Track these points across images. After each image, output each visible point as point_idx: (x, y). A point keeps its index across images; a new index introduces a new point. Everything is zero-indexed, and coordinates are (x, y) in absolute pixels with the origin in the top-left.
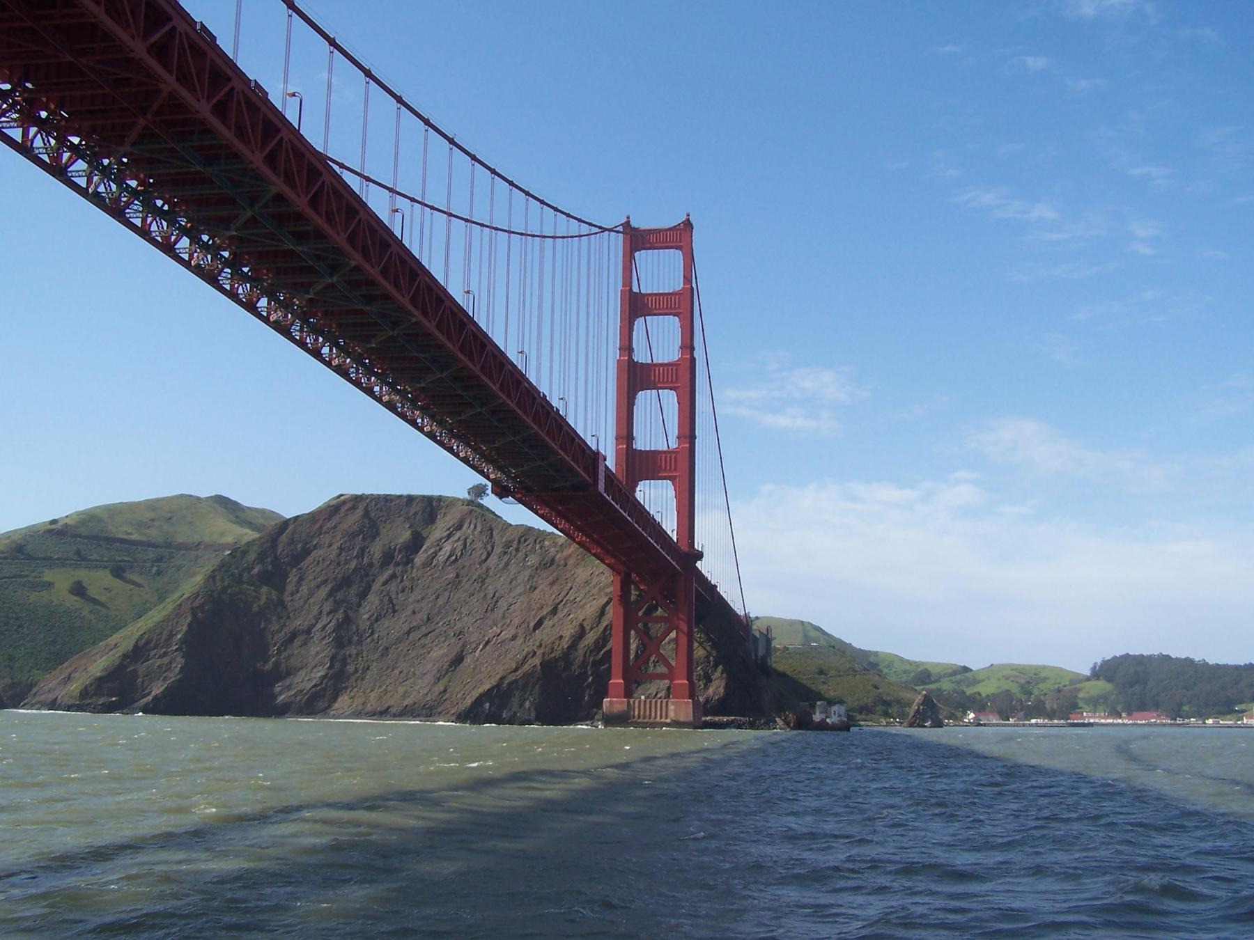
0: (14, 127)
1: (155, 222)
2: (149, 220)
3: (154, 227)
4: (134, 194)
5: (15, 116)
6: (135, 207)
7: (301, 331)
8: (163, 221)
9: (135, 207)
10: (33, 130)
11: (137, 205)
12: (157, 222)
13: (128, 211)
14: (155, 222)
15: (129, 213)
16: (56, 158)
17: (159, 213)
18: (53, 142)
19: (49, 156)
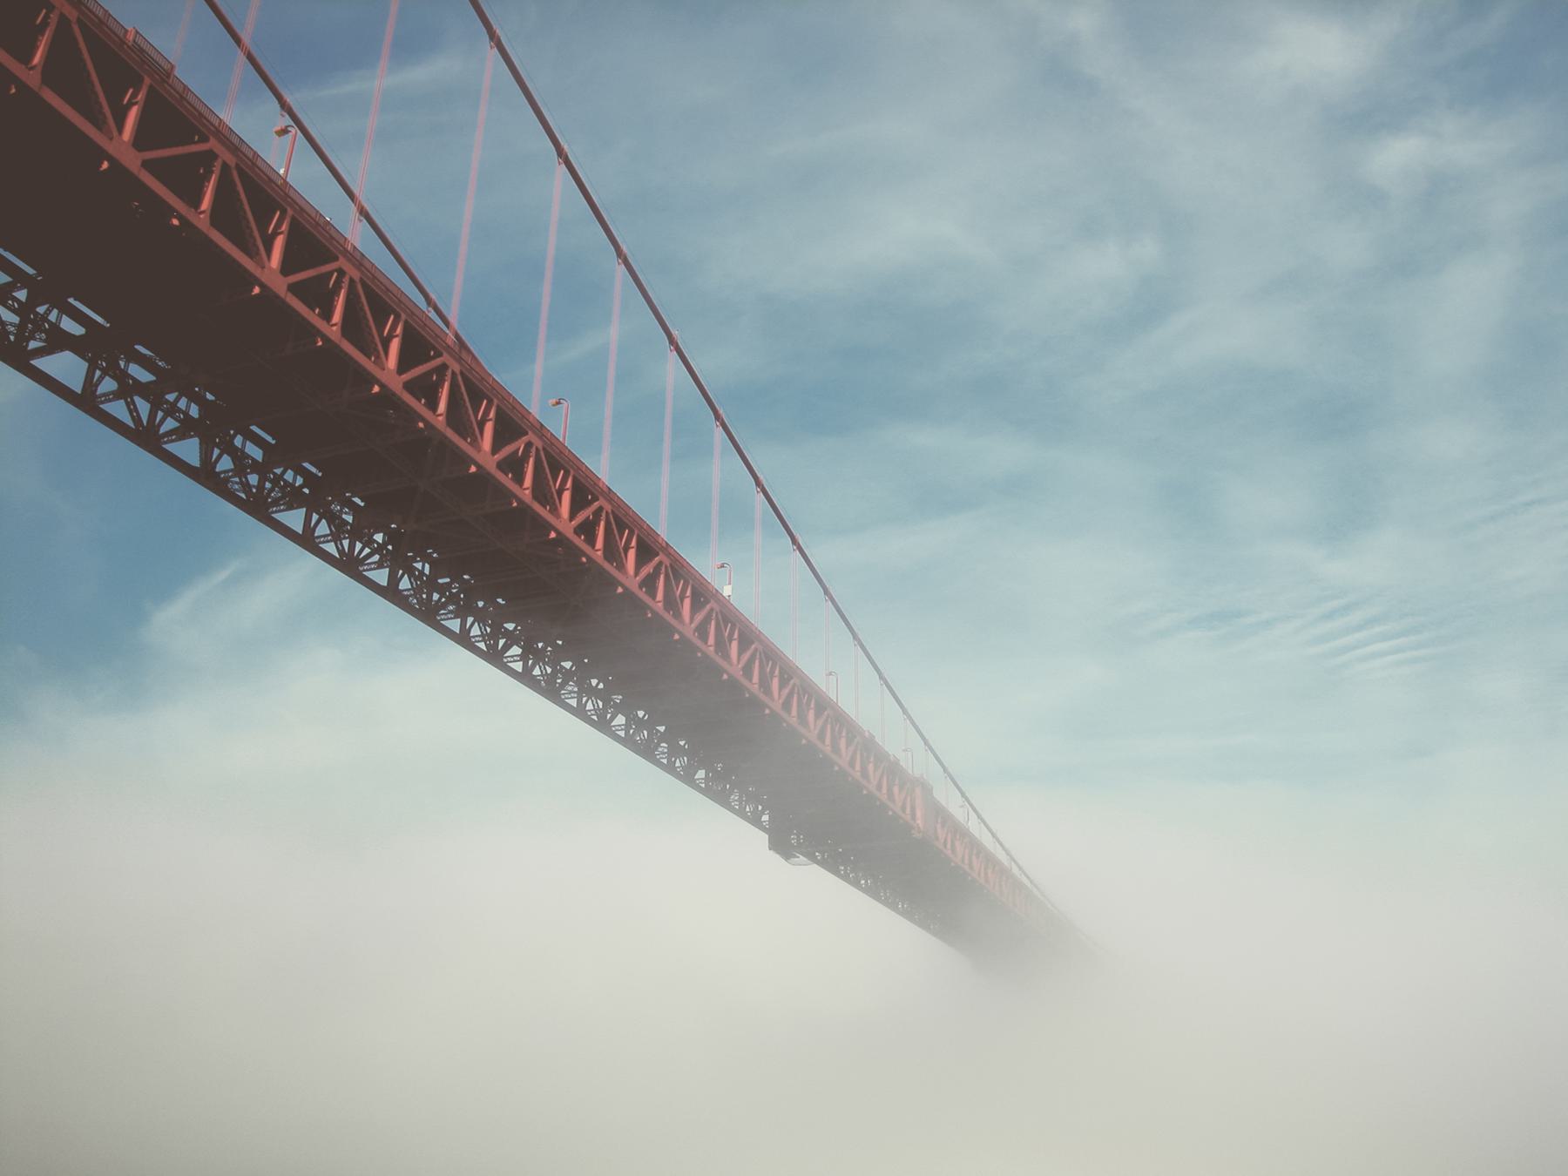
0: (451, 618)
1: (590, 701)
2: (584, 699)
3: (589, 706)
4: (568, 675)
5: (451, 608)
6: (570, 688)
7: (627, 726)
8: (599, 701)
9: (570, 688)
10: (470, 620)
11: (572, 687)
12: (592, 701)
13: (563, 692)
14: (590, 701)
15: (564, 694)
16: (601, 714)
17: (593, 693)
18: (489, 630)
19: (485, 643)
